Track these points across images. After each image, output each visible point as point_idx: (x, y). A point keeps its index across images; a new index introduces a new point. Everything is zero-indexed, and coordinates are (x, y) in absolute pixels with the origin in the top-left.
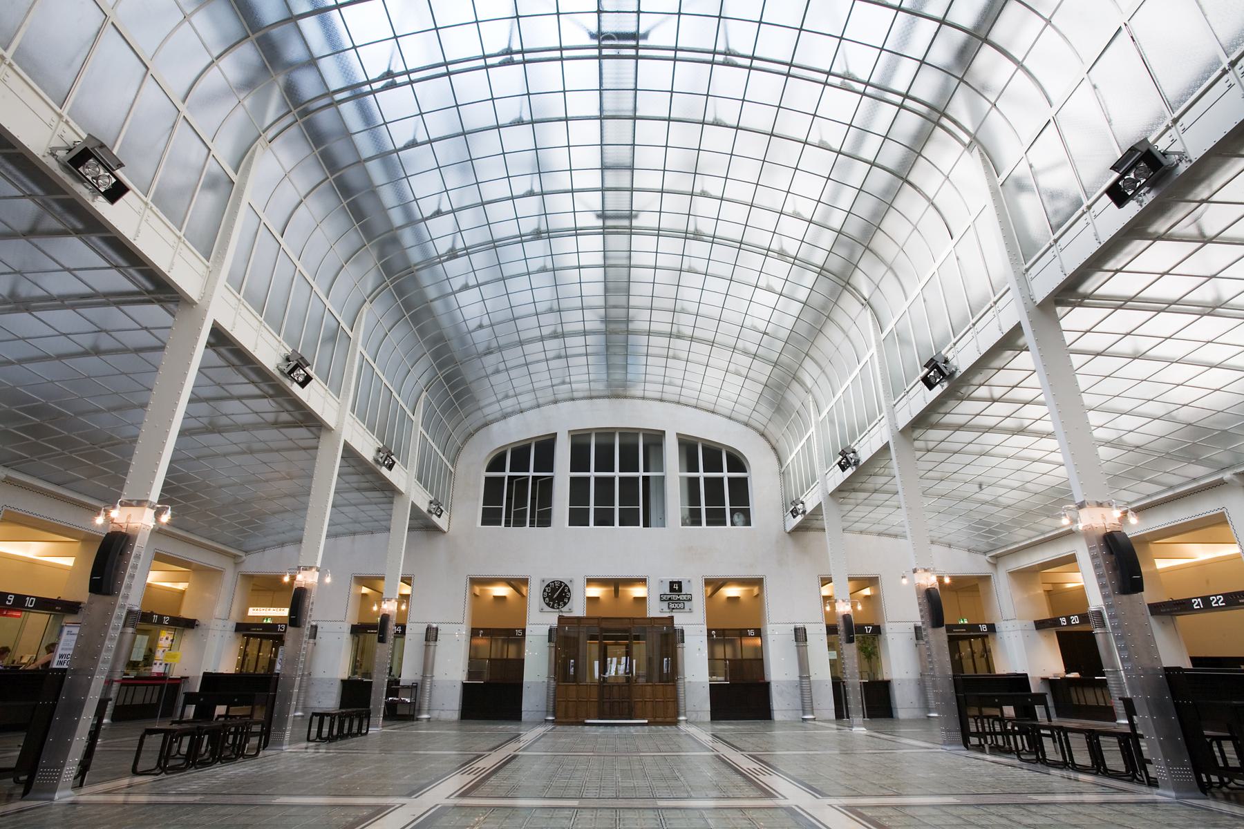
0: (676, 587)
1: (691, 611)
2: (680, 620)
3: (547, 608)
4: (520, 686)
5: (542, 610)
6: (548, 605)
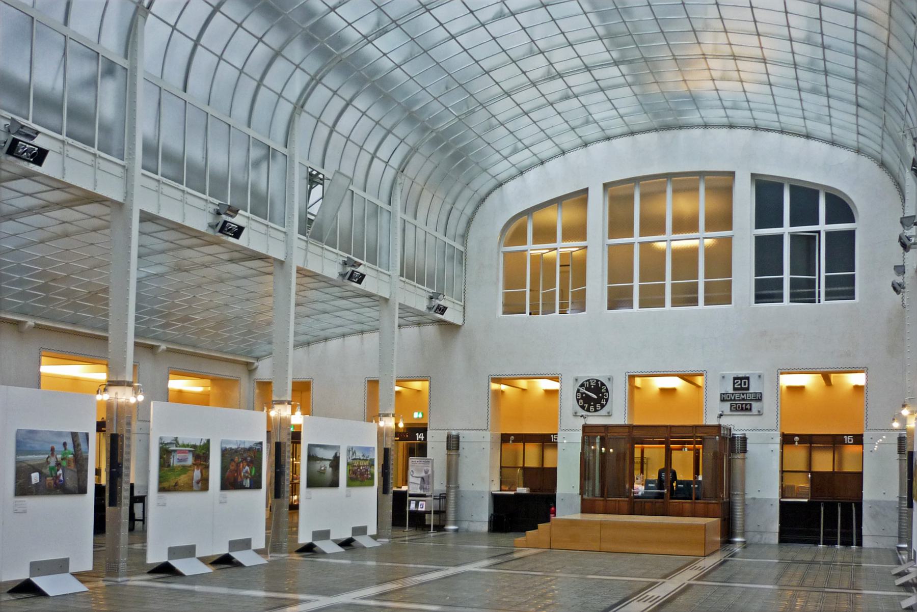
0: (741, 383)
1: (760, 413)
2: (738, 424)
3: (582, 412)
4: (555, 496)
5: (575, 415)
6: (583, 407)
